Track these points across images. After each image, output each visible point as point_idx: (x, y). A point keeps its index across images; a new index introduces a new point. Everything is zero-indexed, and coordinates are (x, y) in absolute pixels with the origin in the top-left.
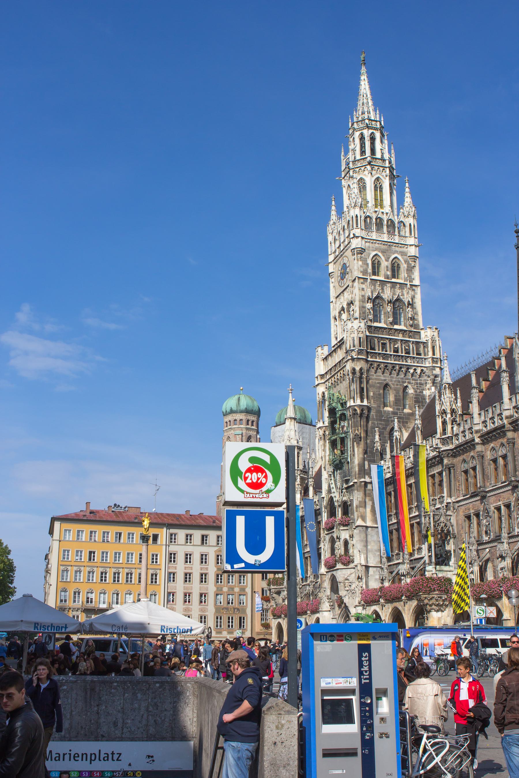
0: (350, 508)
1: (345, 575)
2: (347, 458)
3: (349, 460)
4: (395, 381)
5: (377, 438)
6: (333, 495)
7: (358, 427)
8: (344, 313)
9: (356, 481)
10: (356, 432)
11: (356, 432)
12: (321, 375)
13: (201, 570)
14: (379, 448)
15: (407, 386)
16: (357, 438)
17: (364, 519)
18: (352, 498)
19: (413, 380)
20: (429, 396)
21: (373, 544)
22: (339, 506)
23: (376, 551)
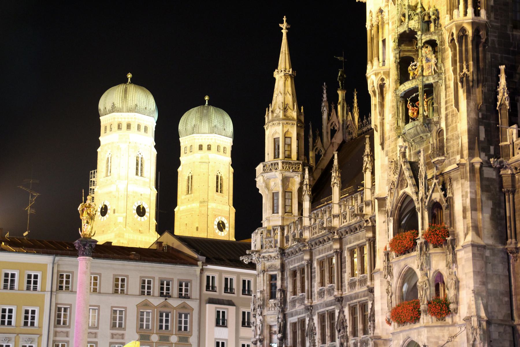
1: (438, 338)
2: (438, 122)
3: (443, 125)
5: (503, 81)
6: (409, 190)
9: (463, 161)
10: (465, 70)
11: (465, 70)
13: (112, 338)
14: (507, 103)
18: (450, 195)
21: (496, 281)
23: (502, 294)
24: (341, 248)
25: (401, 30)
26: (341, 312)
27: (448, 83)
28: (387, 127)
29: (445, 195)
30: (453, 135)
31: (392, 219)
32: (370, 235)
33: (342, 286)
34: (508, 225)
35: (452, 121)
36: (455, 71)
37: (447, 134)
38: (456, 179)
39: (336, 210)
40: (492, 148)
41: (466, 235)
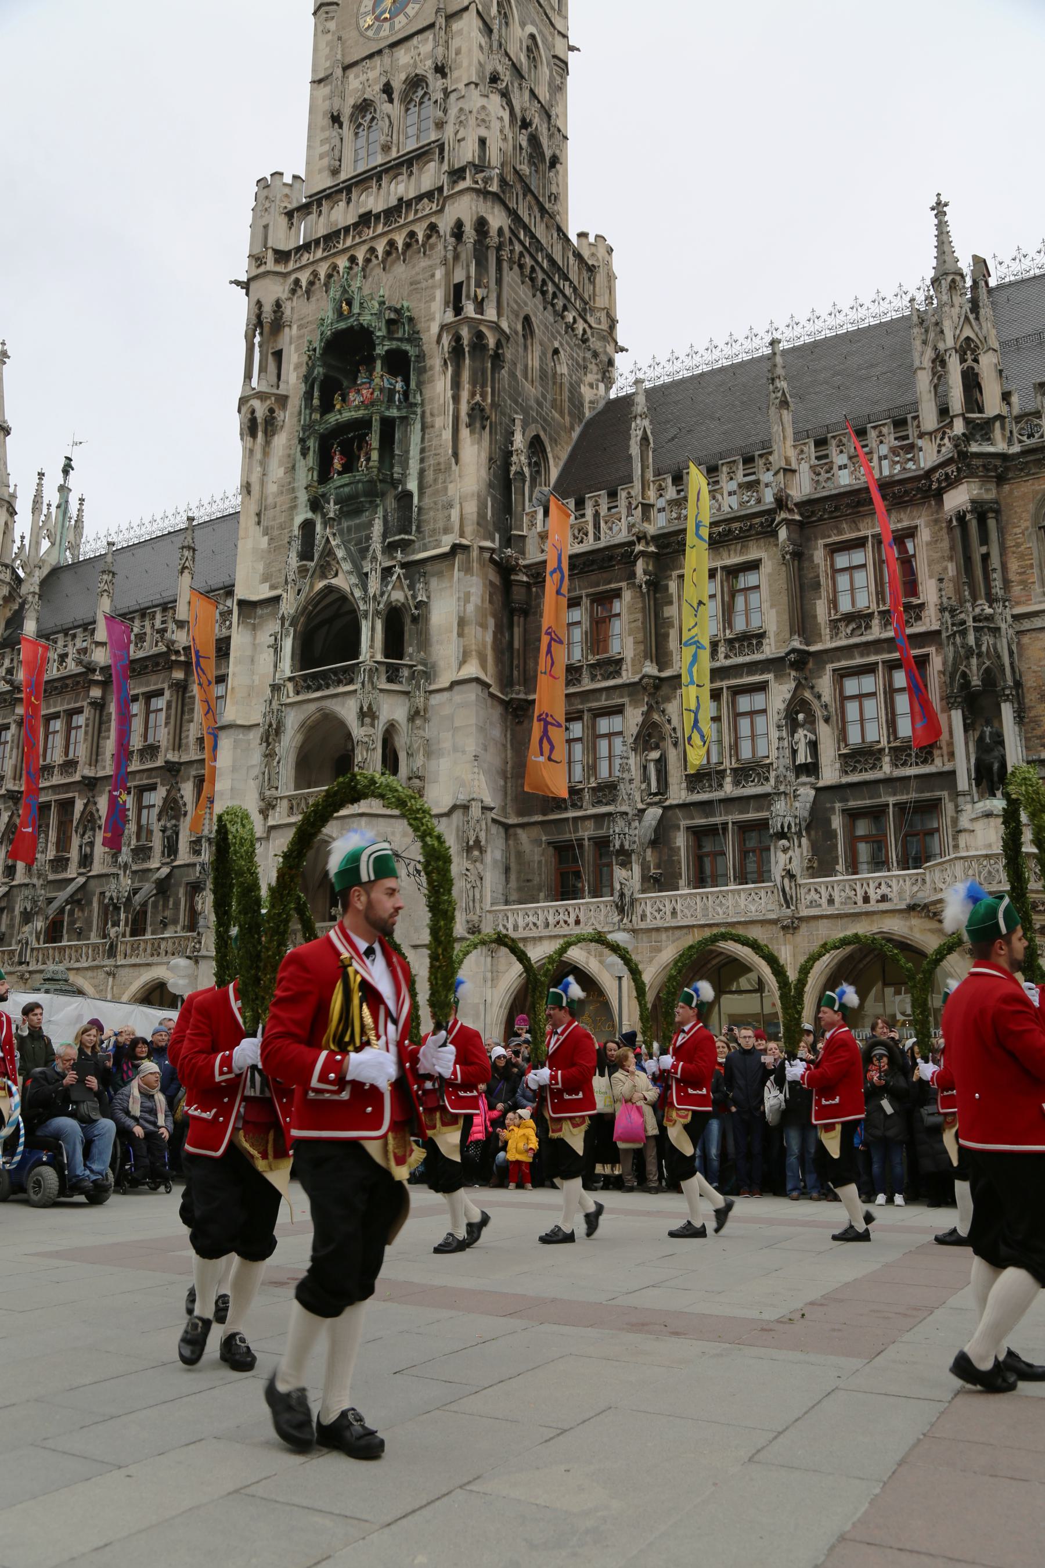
0: (408, 626)
2: (402, 481)
3: (412, 486)
4: (541, 321)
6: (343, 581)
7: (483, 386)
8: (391, 101)
9: (465, 542)
10: (478, 398)
11: (478, 398)
12: (276, 252)
15: (556, 352)
16: (478, 416)
17: (483, 666)
19: (568, 343)
20: (591, 402)
22: (377, 613)
24: (103, 698)
25: (342, 325)
26: (91, 802)
27: (429, 419)
28: (272, 488)
29: (414, 597)
30: (435, 503)
31: (292, 630)
32: (179, 675)
33: (97, 761)
34: (515, 662)
35: (435, 480)
36: (456, 399)
37: (420, 500)
38: (440, 574)
39: (101, 635)
40: (497, 536)
41: (462, 663)
